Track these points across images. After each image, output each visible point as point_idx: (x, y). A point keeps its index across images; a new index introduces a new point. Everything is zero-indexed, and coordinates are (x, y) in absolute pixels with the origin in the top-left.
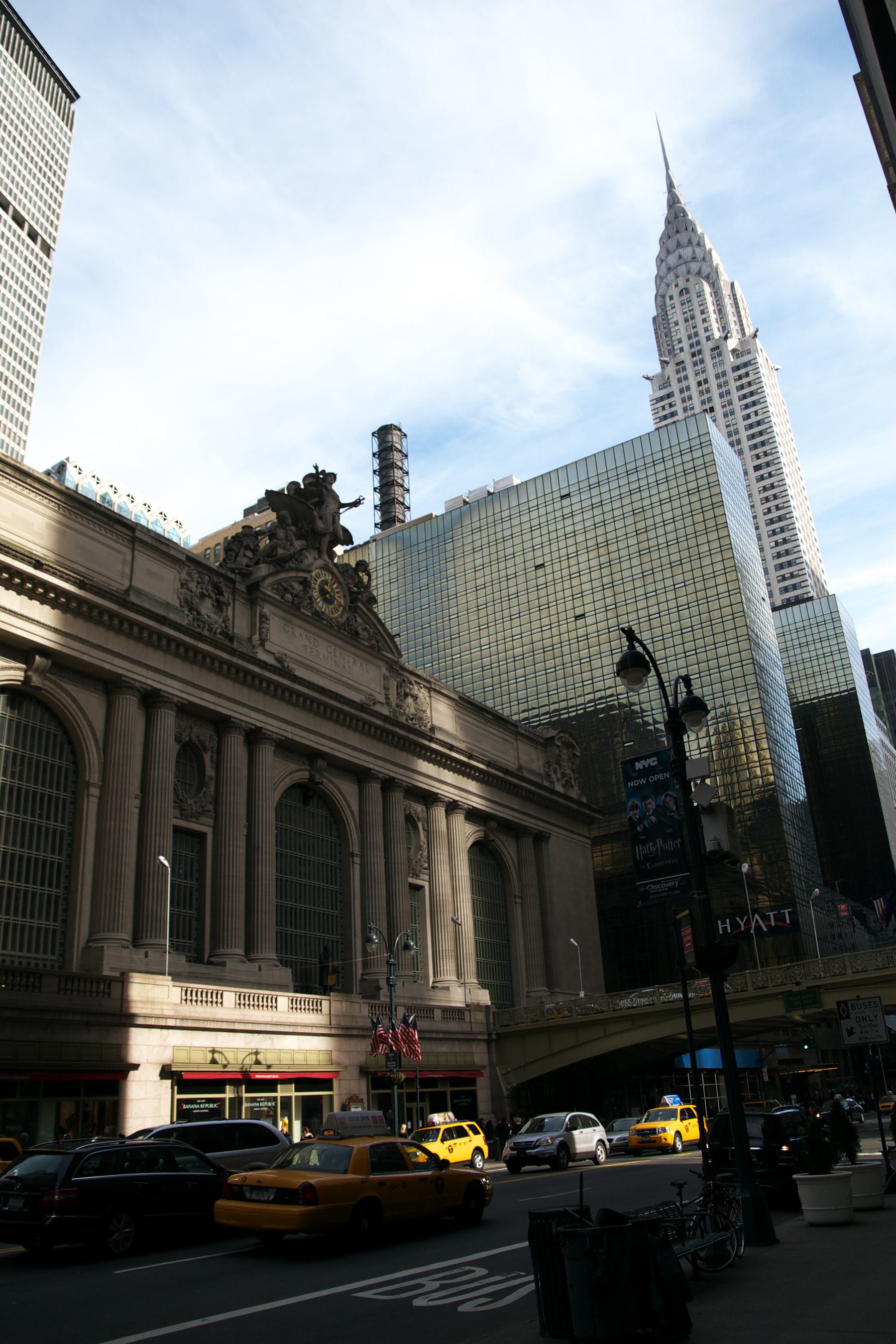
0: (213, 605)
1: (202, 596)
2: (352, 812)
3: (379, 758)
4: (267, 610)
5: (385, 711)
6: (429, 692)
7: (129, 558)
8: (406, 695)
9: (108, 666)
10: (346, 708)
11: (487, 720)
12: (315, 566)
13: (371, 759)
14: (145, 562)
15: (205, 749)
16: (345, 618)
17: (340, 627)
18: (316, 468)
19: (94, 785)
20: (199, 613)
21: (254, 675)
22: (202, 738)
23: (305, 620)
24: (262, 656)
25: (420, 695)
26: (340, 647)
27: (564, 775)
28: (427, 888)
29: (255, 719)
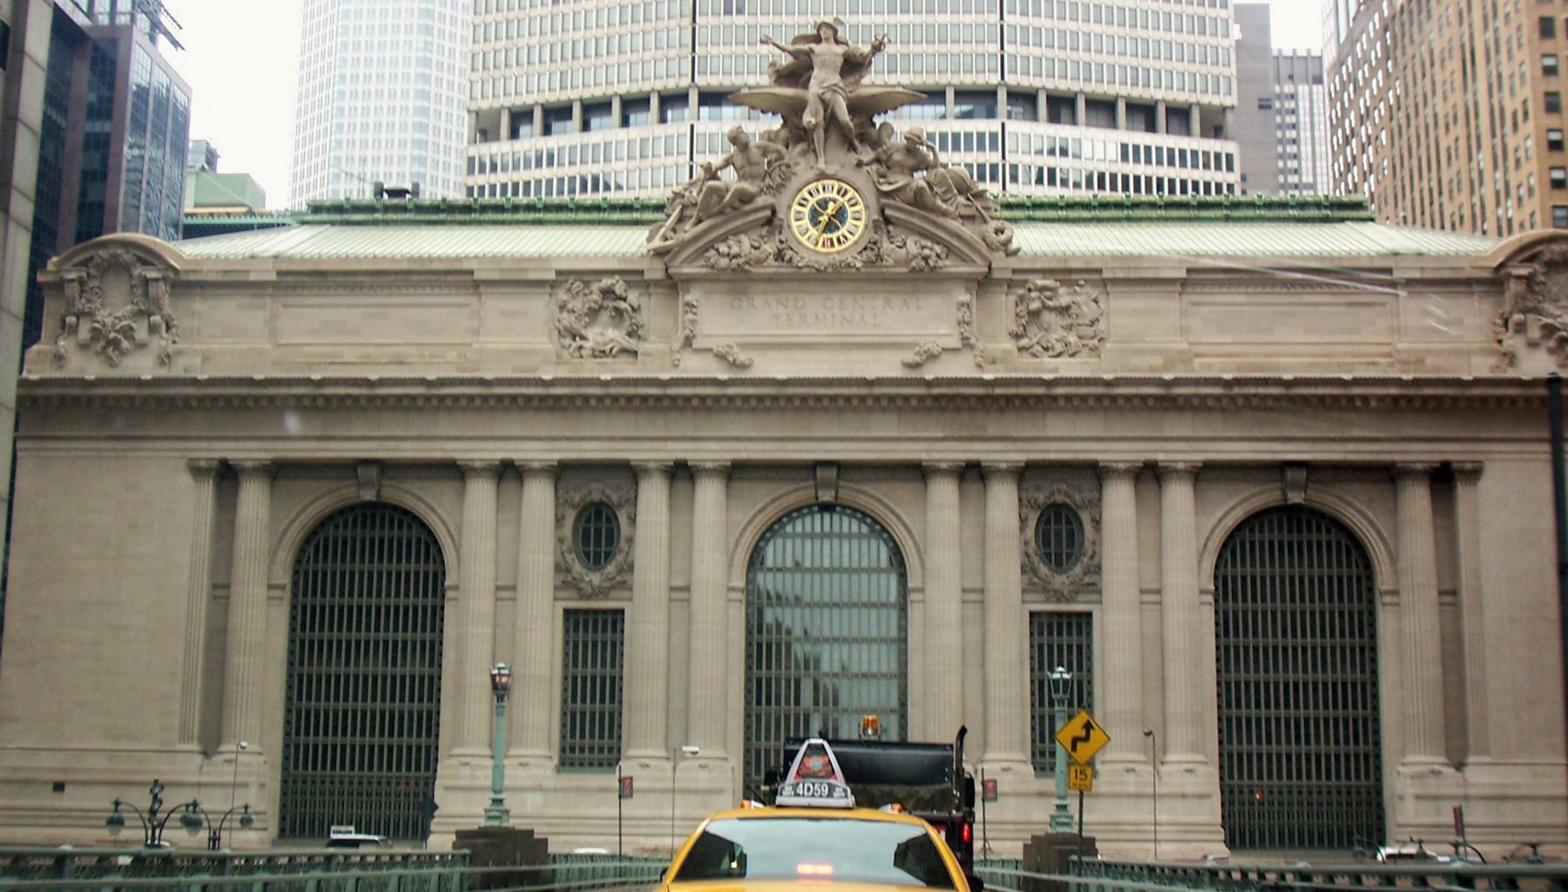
1: (594, 313)
14: (494, 304)
15: (620, 505)
20: (583, 338)
22: (608, 492)
25: (1077, 299)
27: (1549, 330)
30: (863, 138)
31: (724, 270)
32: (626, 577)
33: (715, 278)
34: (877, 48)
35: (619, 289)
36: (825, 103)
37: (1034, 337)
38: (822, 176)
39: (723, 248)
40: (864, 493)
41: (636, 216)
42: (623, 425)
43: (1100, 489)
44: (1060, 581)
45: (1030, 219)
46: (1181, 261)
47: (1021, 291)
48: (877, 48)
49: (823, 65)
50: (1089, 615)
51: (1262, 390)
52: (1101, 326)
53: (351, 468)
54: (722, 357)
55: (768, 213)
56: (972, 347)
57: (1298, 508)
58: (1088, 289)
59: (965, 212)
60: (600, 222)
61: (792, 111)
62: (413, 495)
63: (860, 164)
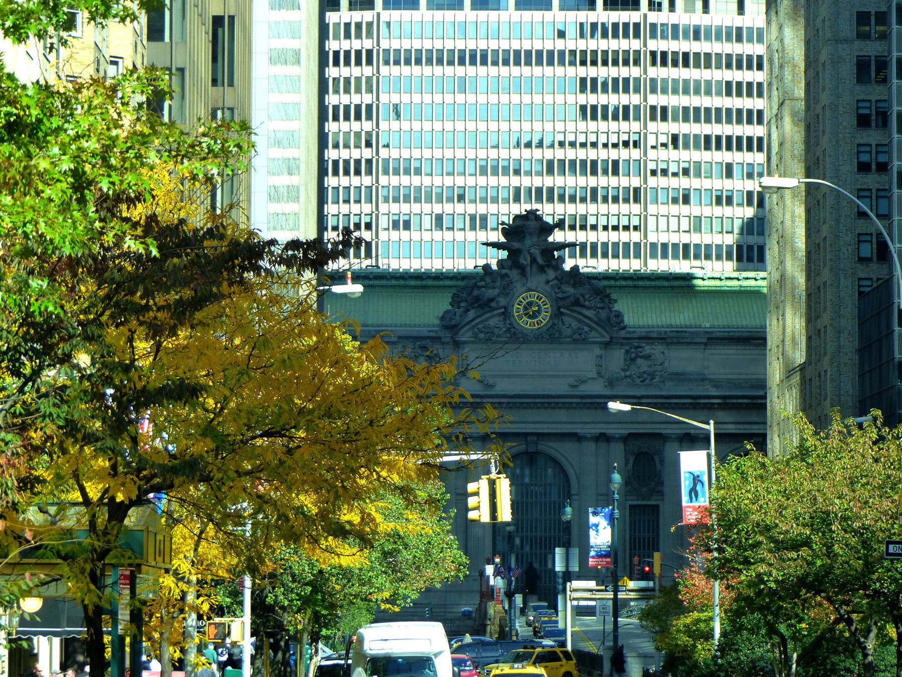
3: (587, 423)
10: (537, 400)
12: (517, 295)
25: (653, 351)
30: (549, 266)
33: (476, 340)
36: (531, 255)
37: (633, 370)
39: (480, 326)
41: (424, 283)
44: (644, 490)
45: (636, 287)
46: (707, 332)
47: (627, 348)
49: (531, 234)
50: (657, 506)
51: (740, 401)
52: (666, 364)
54: (480, 381)
55: (503, 310)
56: (602, 377)
59: (599, 305)
60: (405, 287)
61: (514, 254)
63: (548, 282)
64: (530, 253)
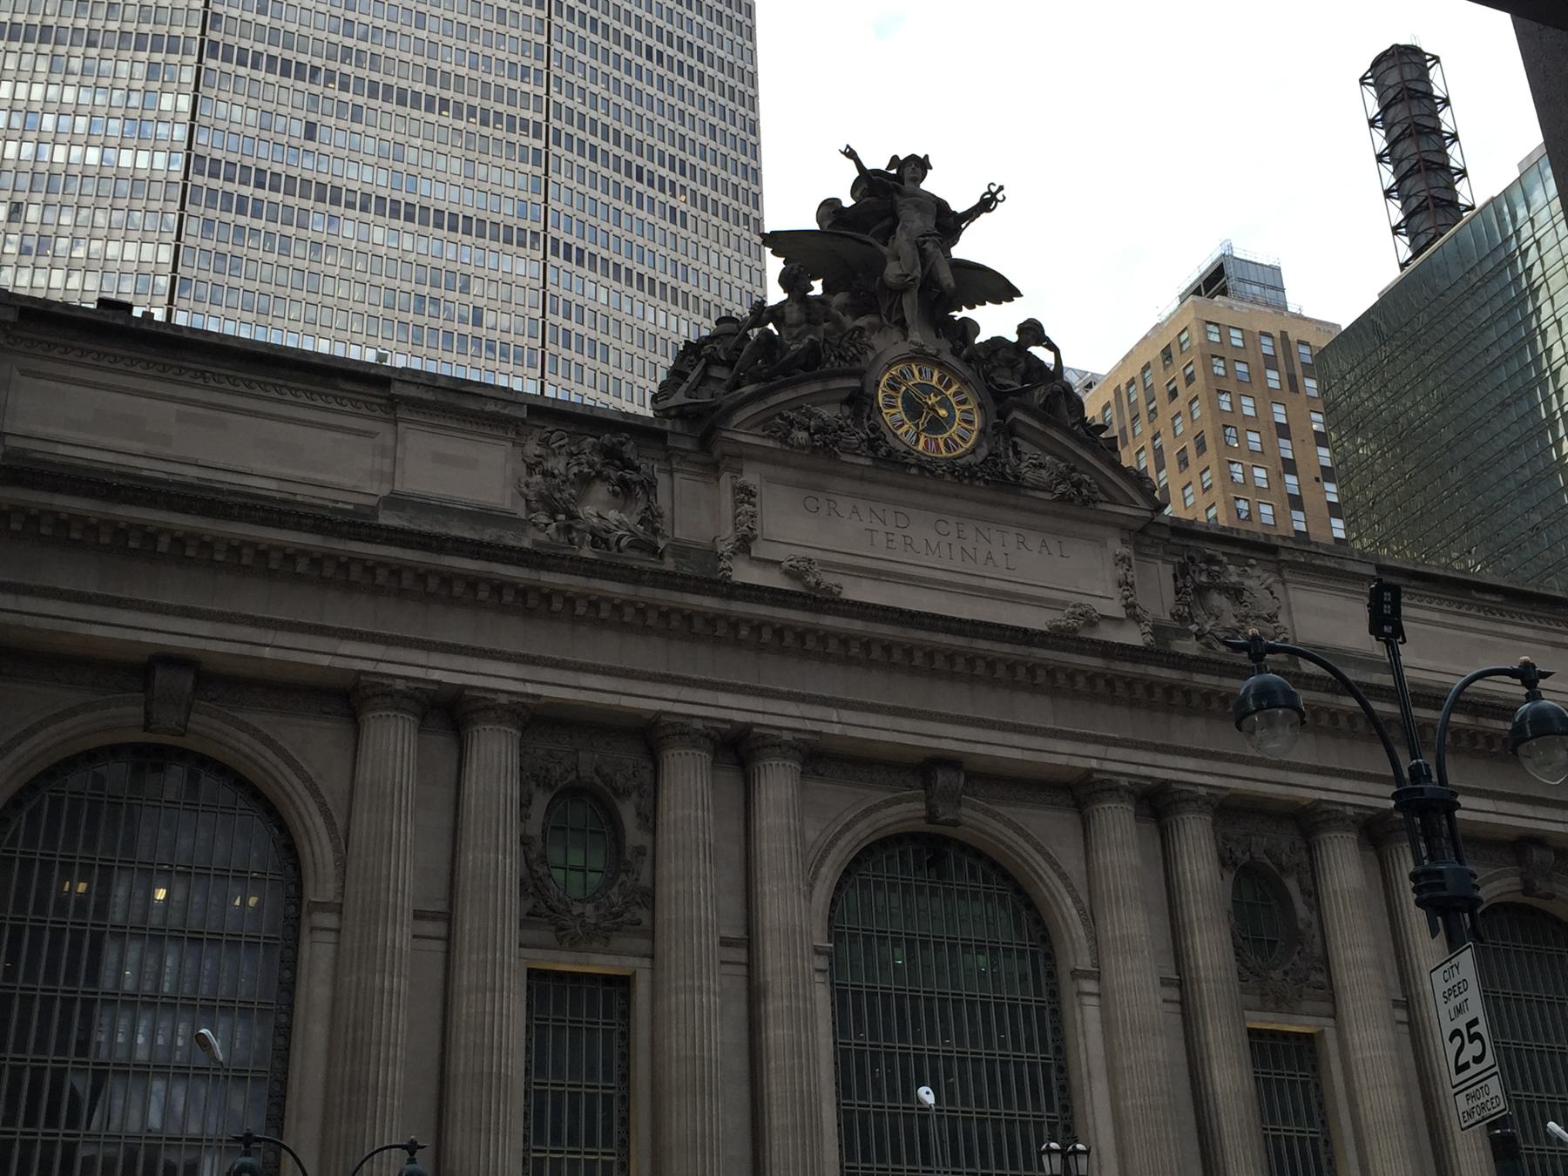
0: (615, 494)
1: (585, 481)
2: (1063, 877)
4: (751, 477)
5: (1133, 637)
6: (1279, 572)
7: (389, 441)
8: (1201, 591)
9: (325, 661)
10: (983, 645)
11: (1488, 610)
12: (885, 359)
13: (1091, 749)
15: (623, 794)
16: (983, 452)
17: (961, 474)
18: (850, 154)
19: (322, 907)
20: (572, 516)
21: (712, 620)
23: (862, 479)
24: (744, 573)
25: (1248, 583)
26: (971, 517)
28: (1330, 1034)
29: (736, 709)
31: (802, 447)
32: (643, 915)
34: (987, 203)
35: (629, 451)
38: (919, 356)
40: (995, 816)
42: (644, 653)
43: (1311, 849)
48: (987, 203)
52: (1283, 619)
53: (144, 671)
55: (854, 383)
57: (1532, 910)
58: (1257, 572)
62: (255, 733)
64: (922, 253)
